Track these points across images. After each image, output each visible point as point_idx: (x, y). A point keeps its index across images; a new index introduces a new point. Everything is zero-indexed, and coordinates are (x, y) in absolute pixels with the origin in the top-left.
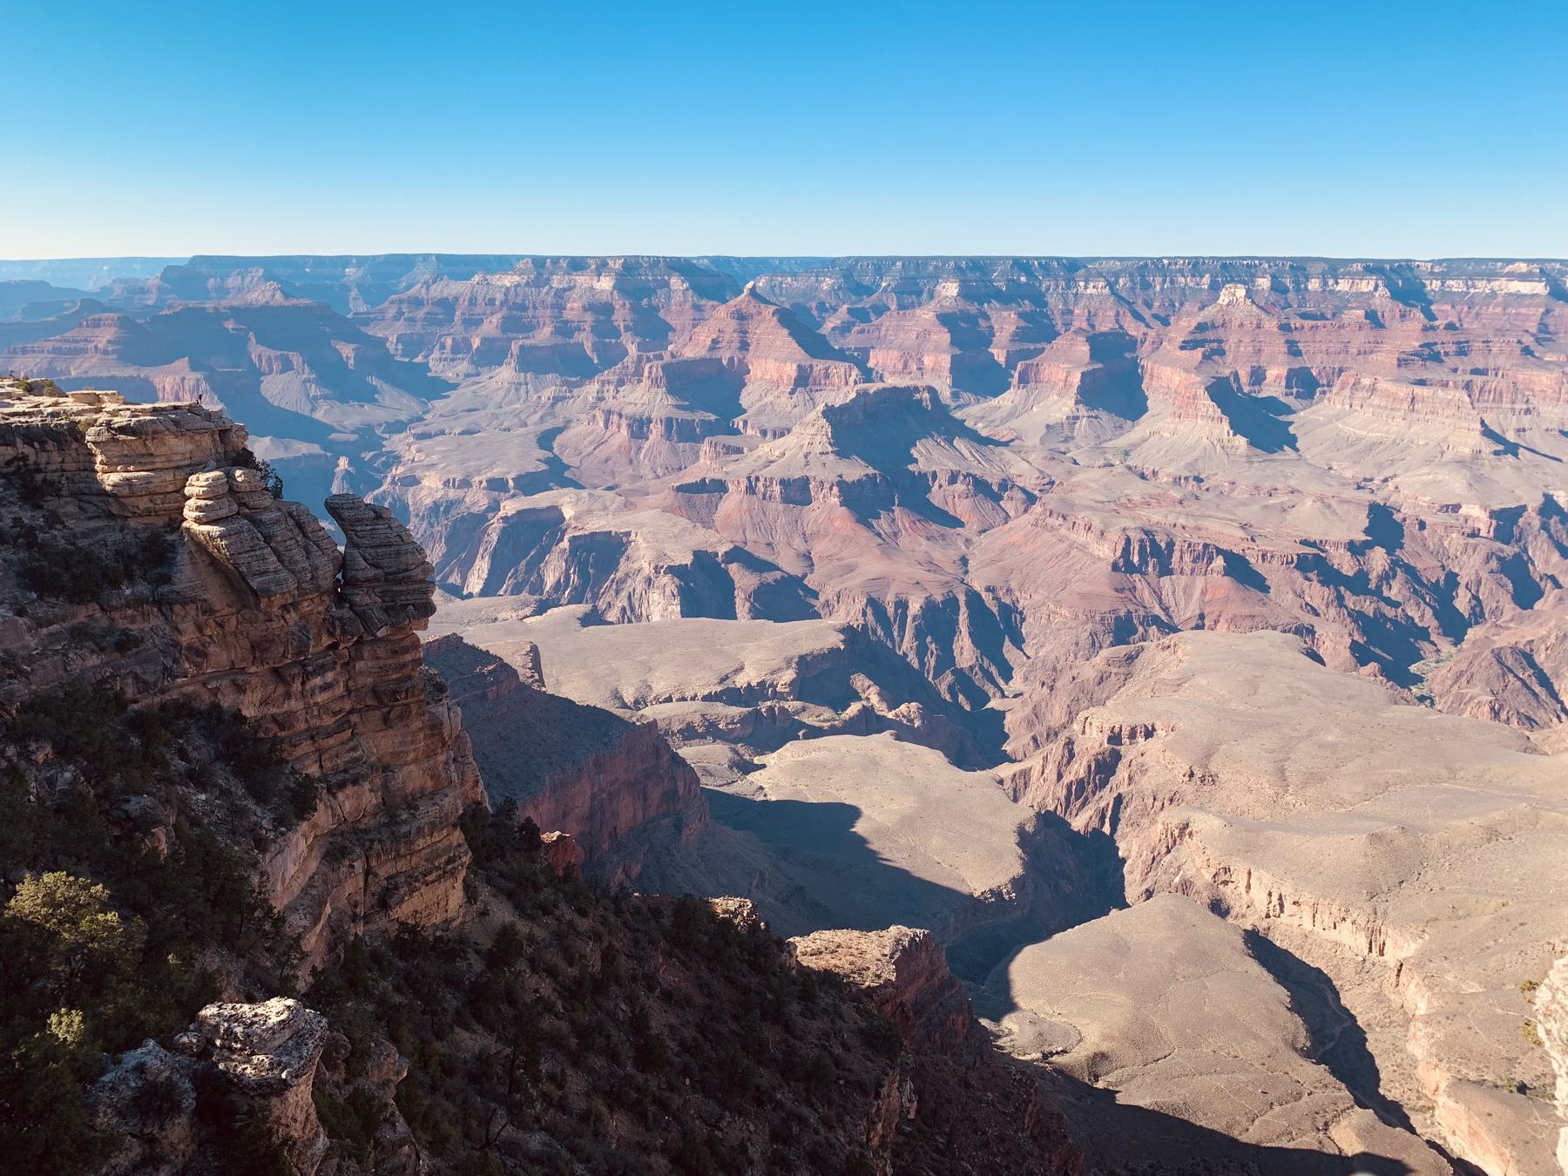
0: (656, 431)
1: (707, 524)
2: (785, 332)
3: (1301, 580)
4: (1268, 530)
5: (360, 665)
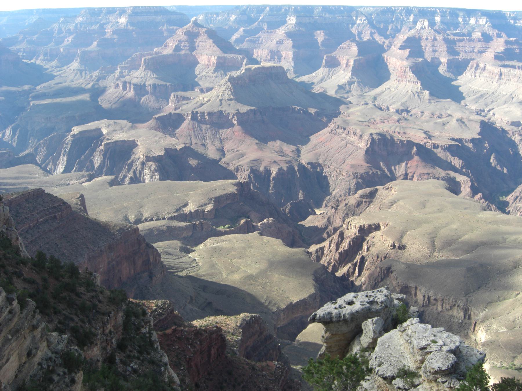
1: (172, 135)
2: (211, 40)
4: (436, 133)
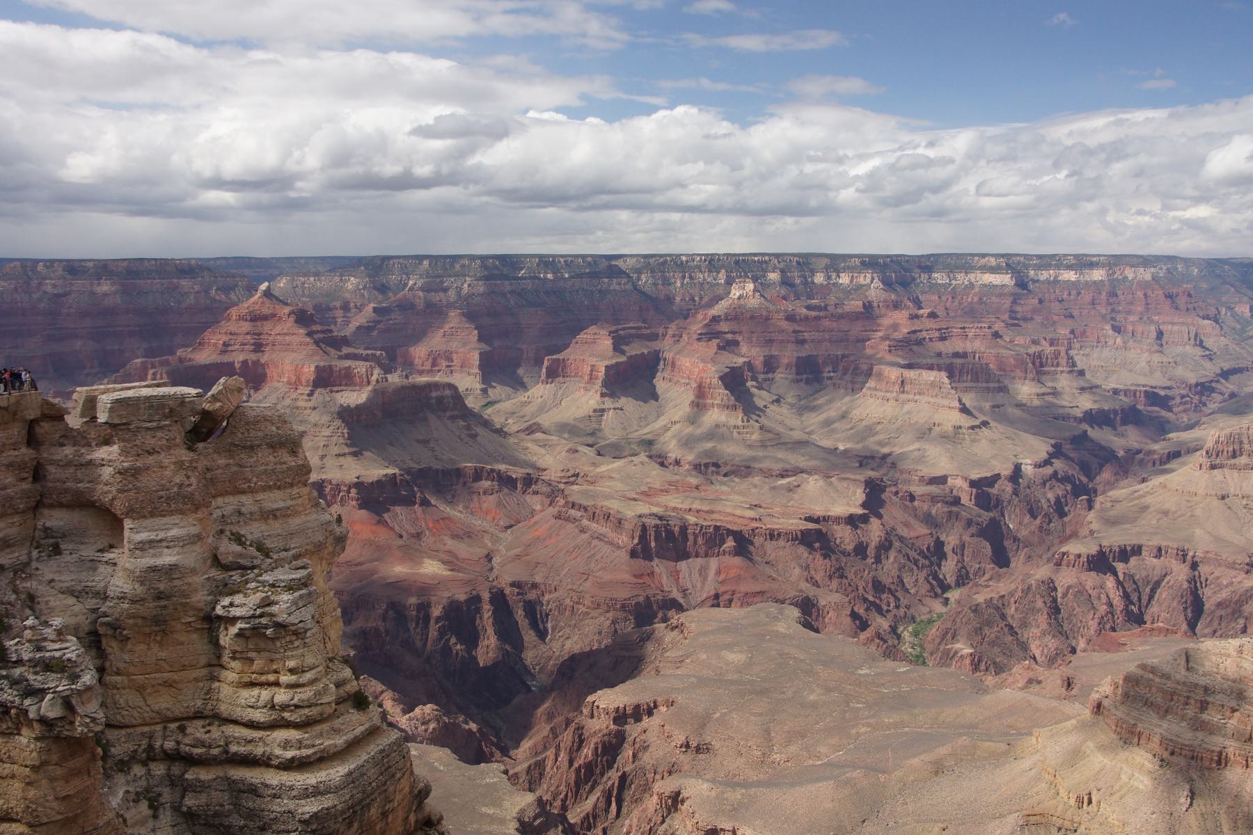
3: (806, 555)
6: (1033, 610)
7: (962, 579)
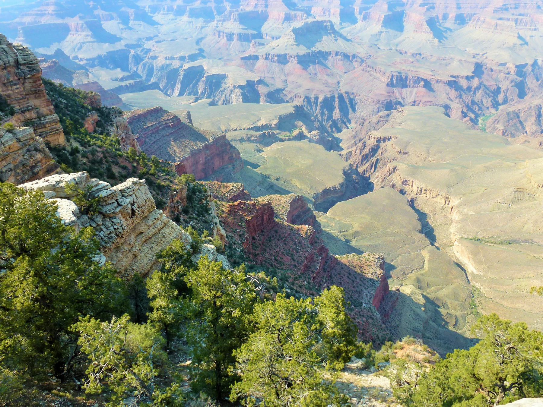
0: (236, 37)
1: (251, 71)
3: (449, 89)
5: (26, 84)
6: (530, 116)
7: (505, 102)
